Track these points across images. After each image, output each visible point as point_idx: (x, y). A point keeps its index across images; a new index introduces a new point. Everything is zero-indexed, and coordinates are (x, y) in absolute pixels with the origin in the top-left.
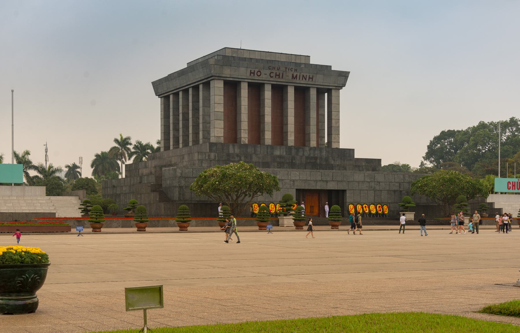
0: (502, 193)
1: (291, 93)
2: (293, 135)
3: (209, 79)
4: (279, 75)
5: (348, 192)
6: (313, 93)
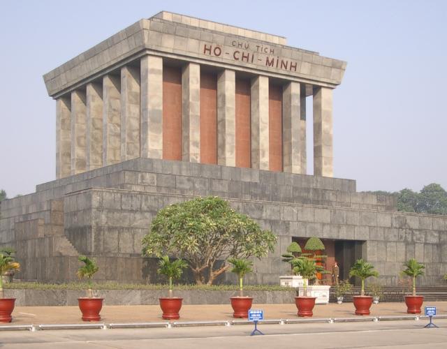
2: (267, 153)
3: (140, 56)
4: (247, 57)
5: (368, 244)
6: (295, 89)
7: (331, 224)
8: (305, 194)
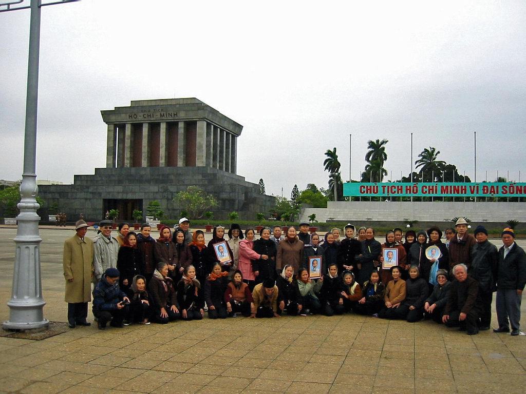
0: (356, 199)
1: (163, 127)
2: (164, 158)
7: (123, 192)
8: (158, 177)
